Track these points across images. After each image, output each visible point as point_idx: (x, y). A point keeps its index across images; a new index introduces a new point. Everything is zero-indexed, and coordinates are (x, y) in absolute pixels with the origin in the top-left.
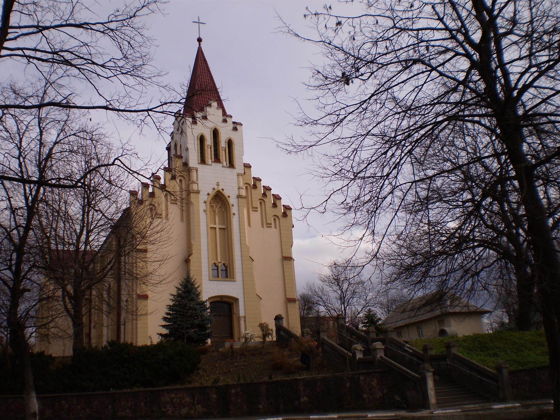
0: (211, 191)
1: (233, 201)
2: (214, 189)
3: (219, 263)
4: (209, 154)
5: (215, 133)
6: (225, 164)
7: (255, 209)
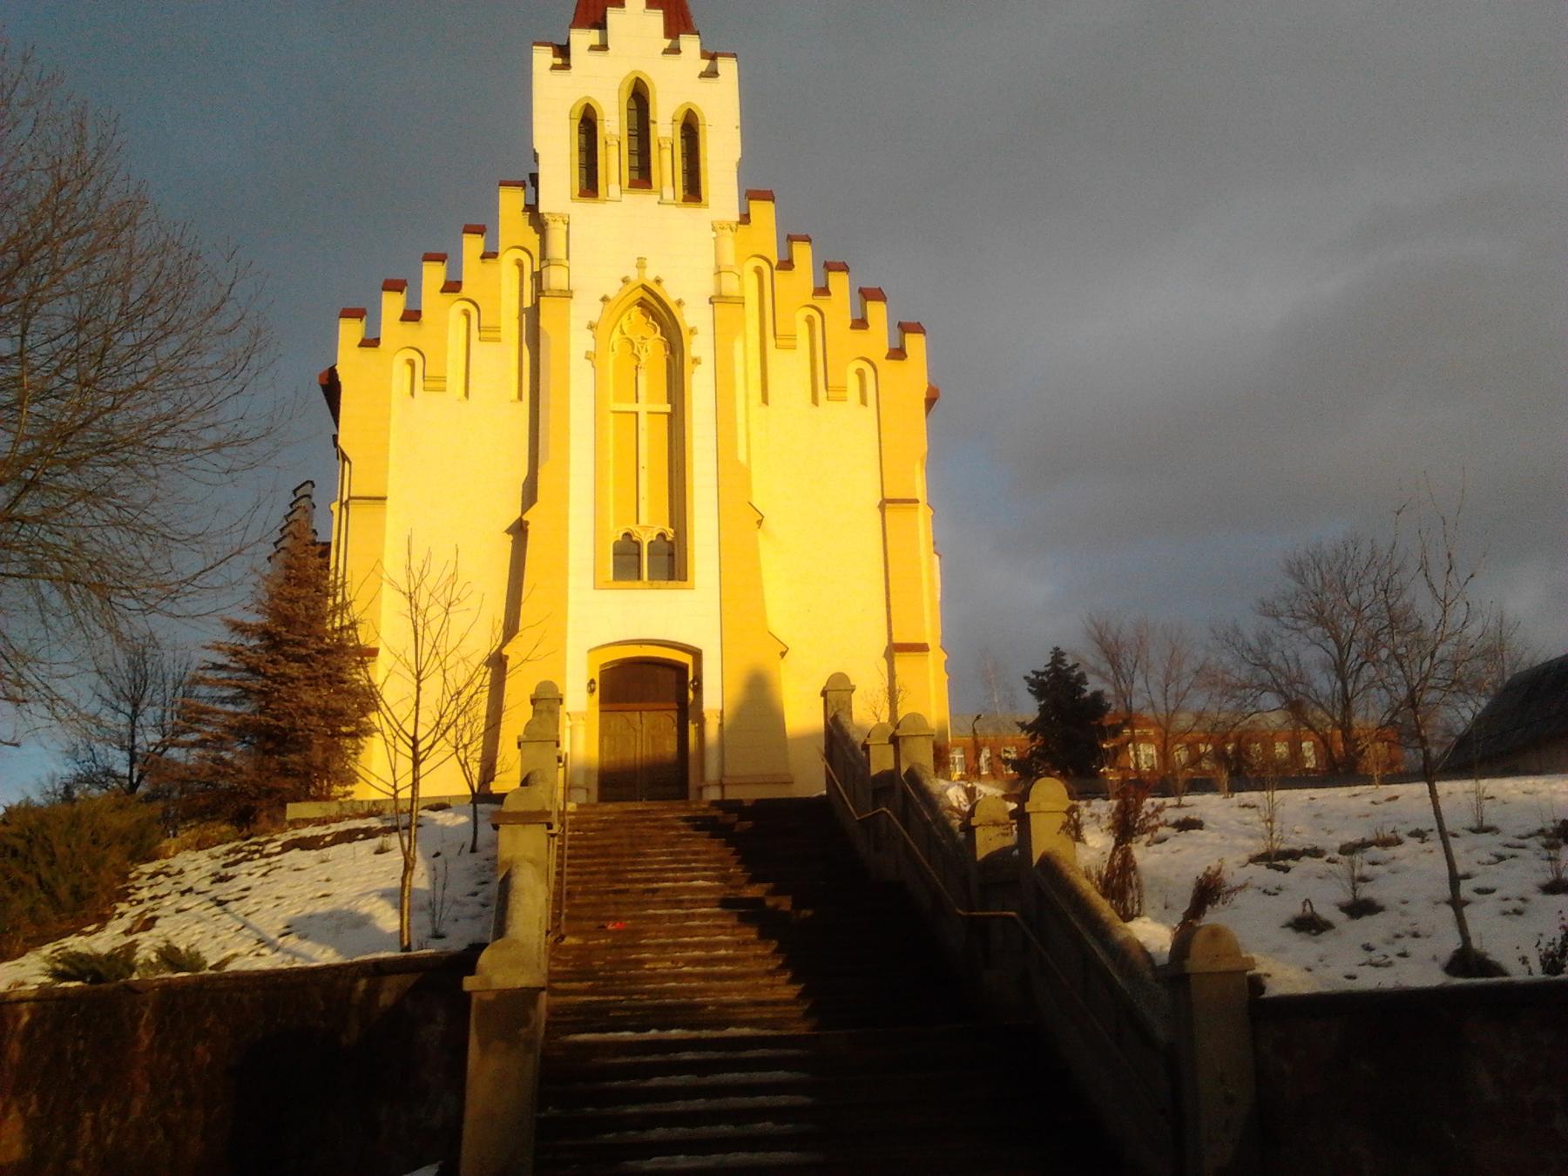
0: (613, 289)
1: (694, 316)
2: (625, 281)
3: (646, 528)
4: (614, 160)
5: (639, 98)
6: (668, 193)
7: (786, 341)
